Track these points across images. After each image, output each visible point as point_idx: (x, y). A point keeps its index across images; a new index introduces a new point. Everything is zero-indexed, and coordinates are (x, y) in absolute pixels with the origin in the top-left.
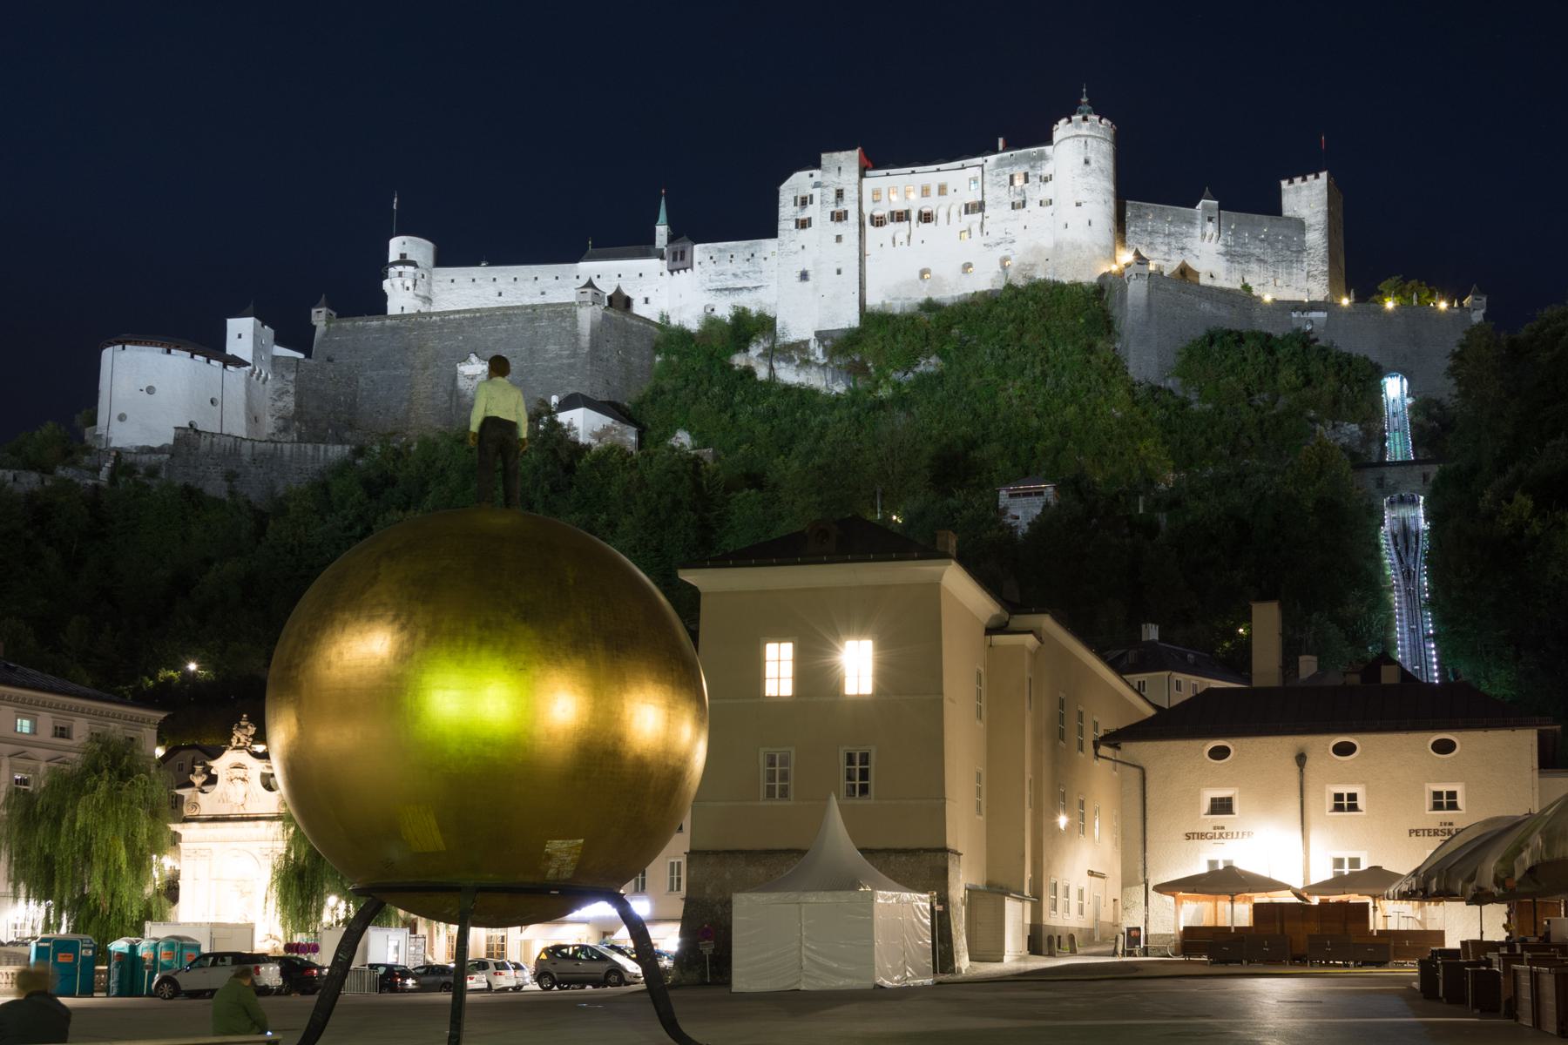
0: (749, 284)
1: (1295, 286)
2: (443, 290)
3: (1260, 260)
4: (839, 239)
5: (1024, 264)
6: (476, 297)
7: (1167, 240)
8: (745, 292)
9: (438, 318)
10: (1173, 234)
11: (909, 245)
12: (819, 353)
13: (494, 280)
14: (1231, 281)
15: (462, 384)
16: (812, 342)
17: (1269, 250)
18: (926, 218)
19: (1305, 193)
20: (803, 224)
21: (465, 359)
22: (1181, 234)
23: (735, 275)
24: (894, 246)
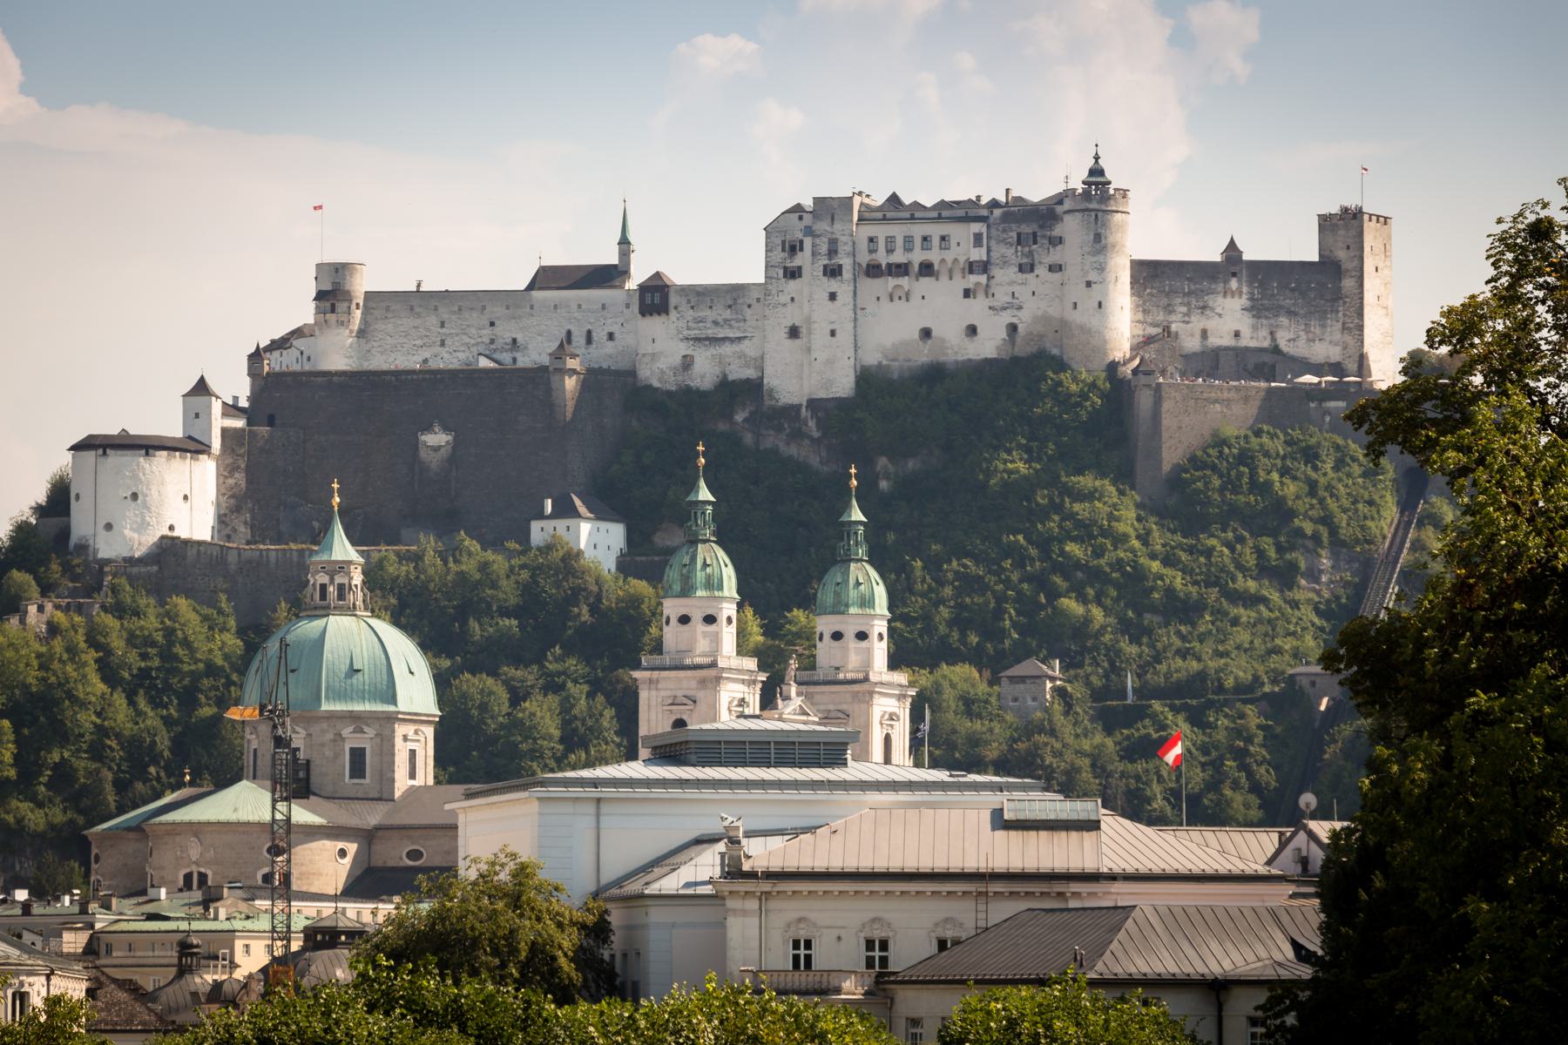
0: (731, 335)
1: (1328, 339)
2: (377, 319)
3: (1291, 313)
4: (833, 297)
5: (1031, 334)
6: (415, 327)
7: (1186, 300)
8: (727, 344)
9: (393, 378)
10: (1194, 293)
11: (907, 300)
12: (812, 424)
13: (436, 309)
14: (1257, 340)
15: (423, 454)
16: (804, 410)
17: (1300, 301)
18: (927, 269)
19: (1342, 232)
20: (793, 274)
21: (428, 428)
22: (1202, 291)
23: (716, 323)
24: (892, 300)
